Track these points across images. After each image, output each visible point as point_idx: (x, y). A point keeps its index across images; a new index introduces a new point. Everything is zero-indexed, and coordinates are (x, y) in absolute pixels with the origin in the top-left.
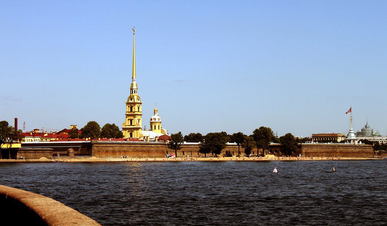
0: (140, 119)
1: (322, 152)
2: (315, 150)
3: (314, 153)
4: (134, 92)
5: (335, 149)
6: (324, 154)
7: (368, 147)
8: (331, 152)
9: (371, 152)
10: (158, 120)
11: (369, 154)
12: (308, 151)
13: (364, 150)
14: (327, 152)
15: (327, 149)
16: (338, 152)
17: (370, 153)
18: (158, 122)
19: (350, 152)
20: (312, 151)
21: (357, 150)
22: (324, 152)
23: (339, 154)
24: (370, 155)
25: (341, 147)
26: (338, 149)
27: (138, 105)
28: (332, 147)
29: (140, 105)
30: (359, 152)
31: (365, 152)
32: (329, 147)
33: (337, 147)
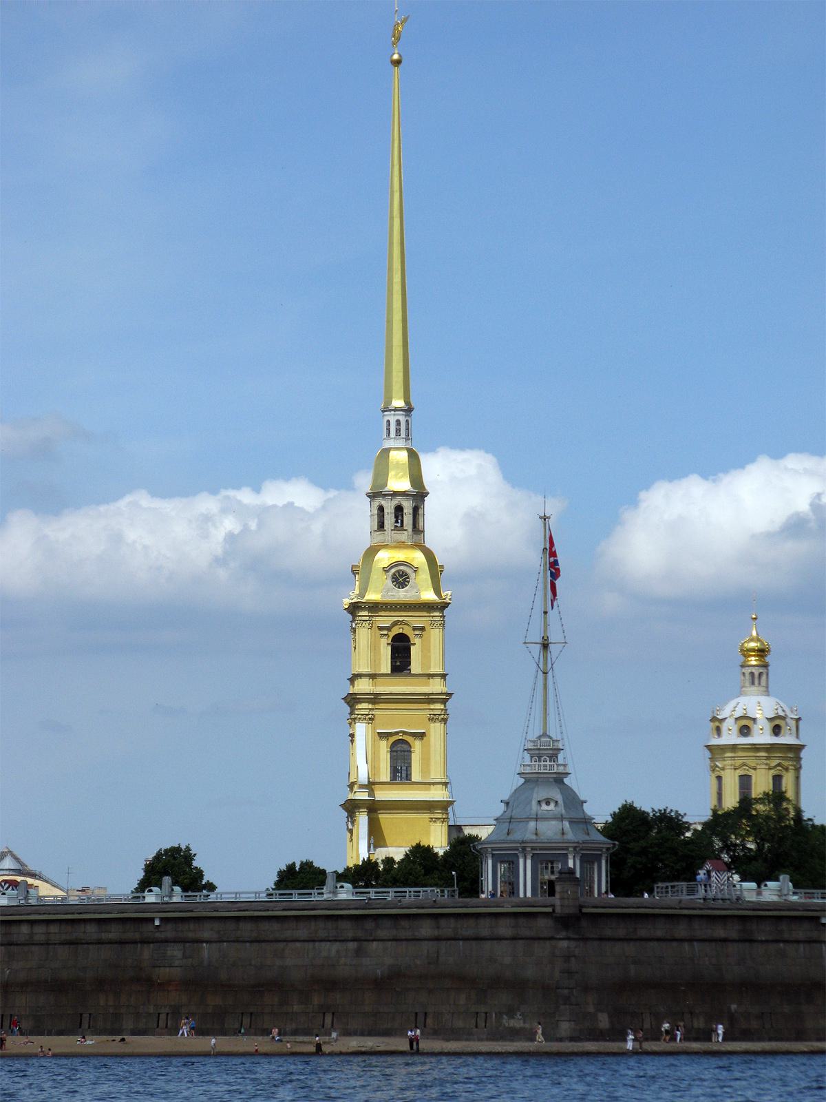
0: (421, 736)
4: (389, 520)
5: (147, 953)
7: (505, 928)
8: (101, 984)
9: (530, 972)
10: (768, 727)
14: (58, 987)
15: (63, 952)
17: (518, 986)
18: (734, 748)
21: (381, 956)
22: (25, 986)
24: (511, 1013)
26: (175, 952)
27: (385, 620)
28: (114, 933)
29: (417, 620)
31: (462, 981)
32: (79, 933)
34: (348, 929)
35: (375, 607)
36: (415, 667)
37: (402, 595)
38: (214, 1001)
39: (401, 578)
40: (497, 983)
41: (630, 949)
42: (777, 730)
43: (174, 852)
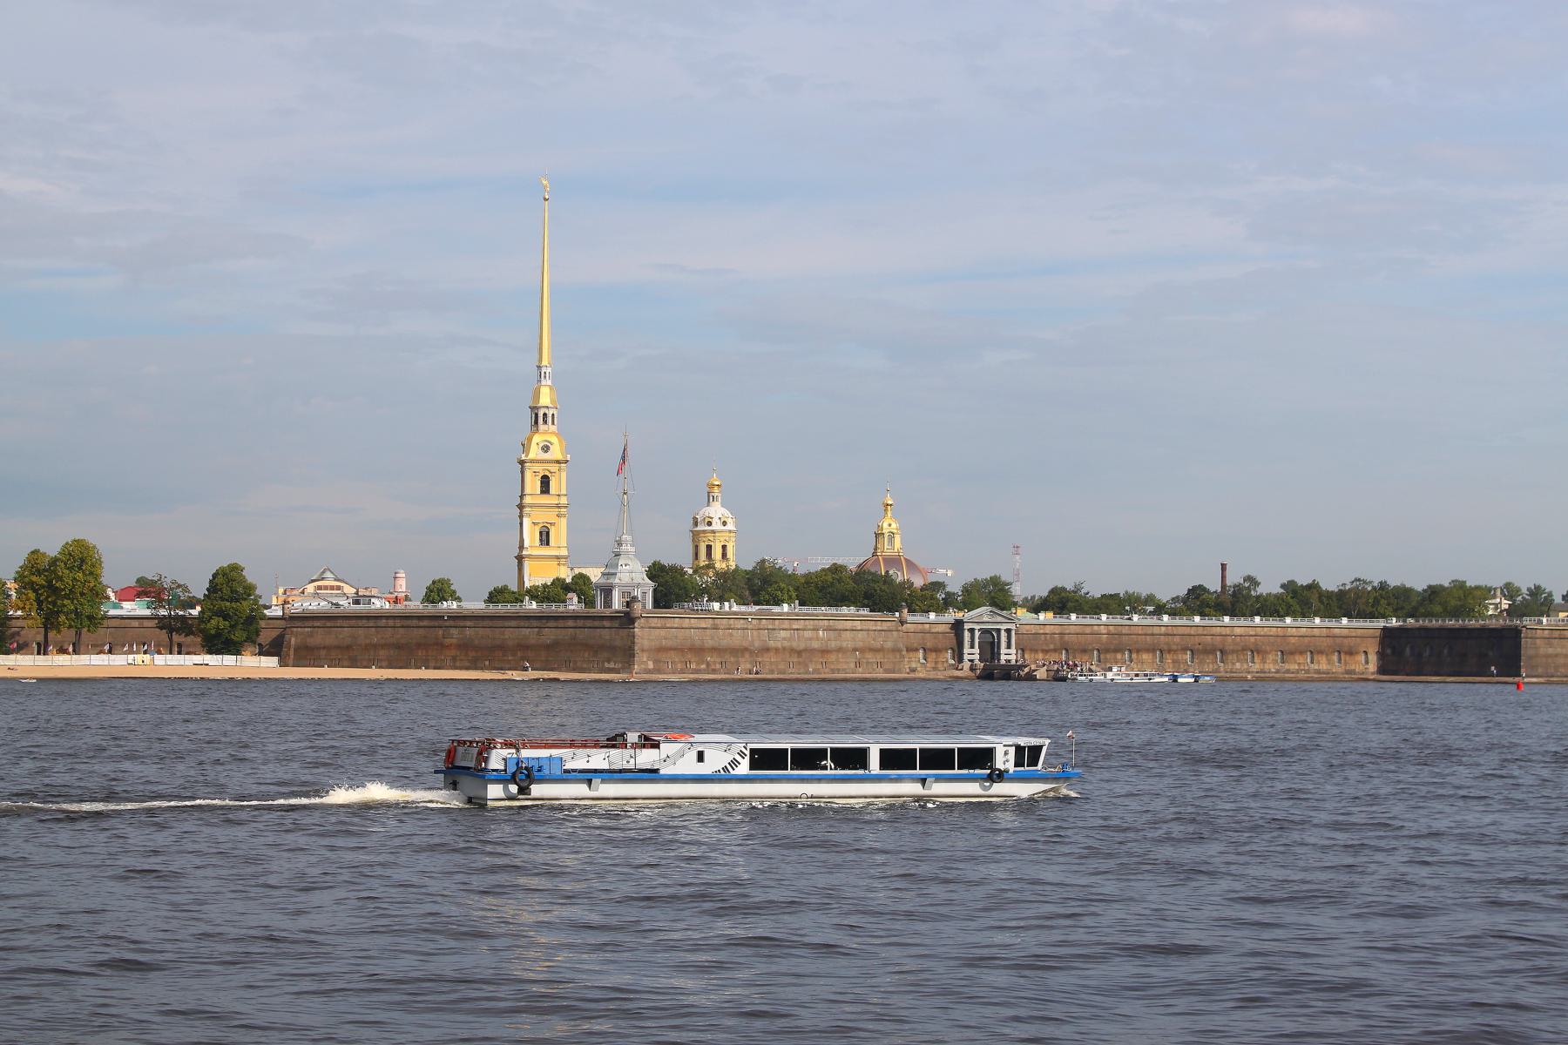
1: (375, 646)
2: (344, 634)
3: (338, 647)
5: (441, 632)
6: (382, 653)
7: (606, 623)
8: (419, 645)
9: (618, 643)
11: (606, 655)
12: (311, 642)
13: (583, 634)
14: (399, 647)
16: (449, 647)
19: (510, 643)
20: (330, 640)
21: (549, 635)
22: (383, 646)
23: (453, 652)
25: (468, 623)
26: (454, 631)
27: (537, 467)
28: (425, 623)
29: (554, 467)
30: (552, 647)
31: (587, 646)
32: (409, 623)
33: (451, 623)
34: (535, 623)
35: (532, 461)
36: (552, 491)
37: (547, 456)
38: (472, 654)
39: (546, 449)
40: (602, 647)
41: (663, 632)
42: (725, 523)
43: (441, 581)
